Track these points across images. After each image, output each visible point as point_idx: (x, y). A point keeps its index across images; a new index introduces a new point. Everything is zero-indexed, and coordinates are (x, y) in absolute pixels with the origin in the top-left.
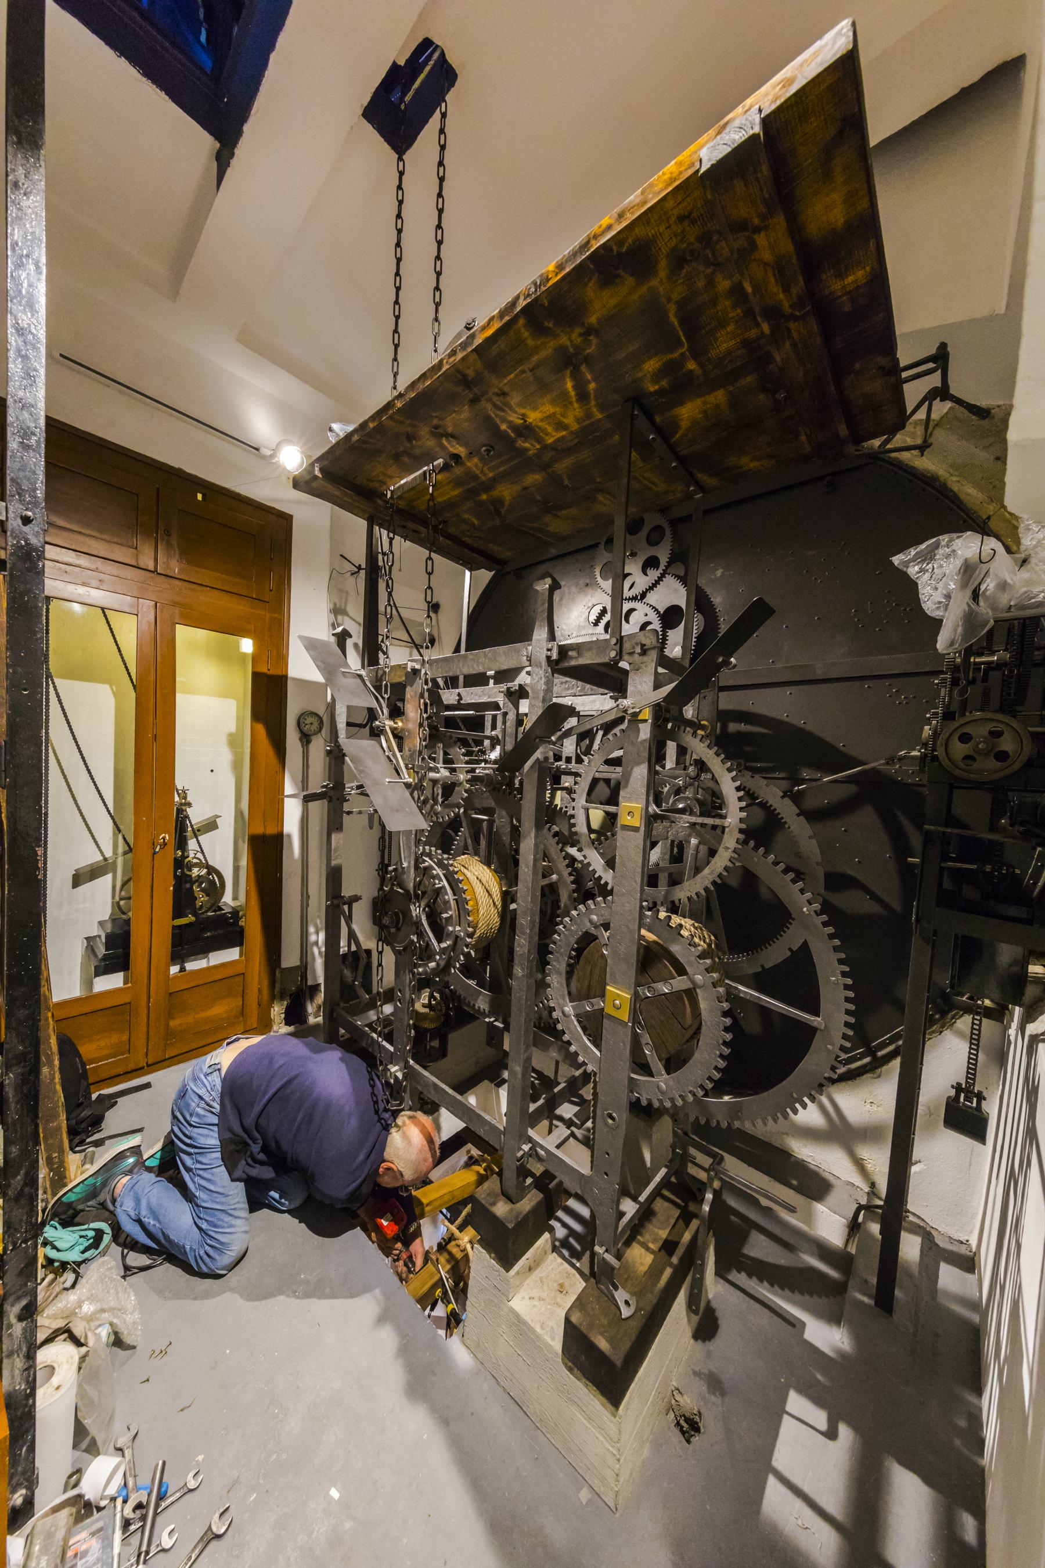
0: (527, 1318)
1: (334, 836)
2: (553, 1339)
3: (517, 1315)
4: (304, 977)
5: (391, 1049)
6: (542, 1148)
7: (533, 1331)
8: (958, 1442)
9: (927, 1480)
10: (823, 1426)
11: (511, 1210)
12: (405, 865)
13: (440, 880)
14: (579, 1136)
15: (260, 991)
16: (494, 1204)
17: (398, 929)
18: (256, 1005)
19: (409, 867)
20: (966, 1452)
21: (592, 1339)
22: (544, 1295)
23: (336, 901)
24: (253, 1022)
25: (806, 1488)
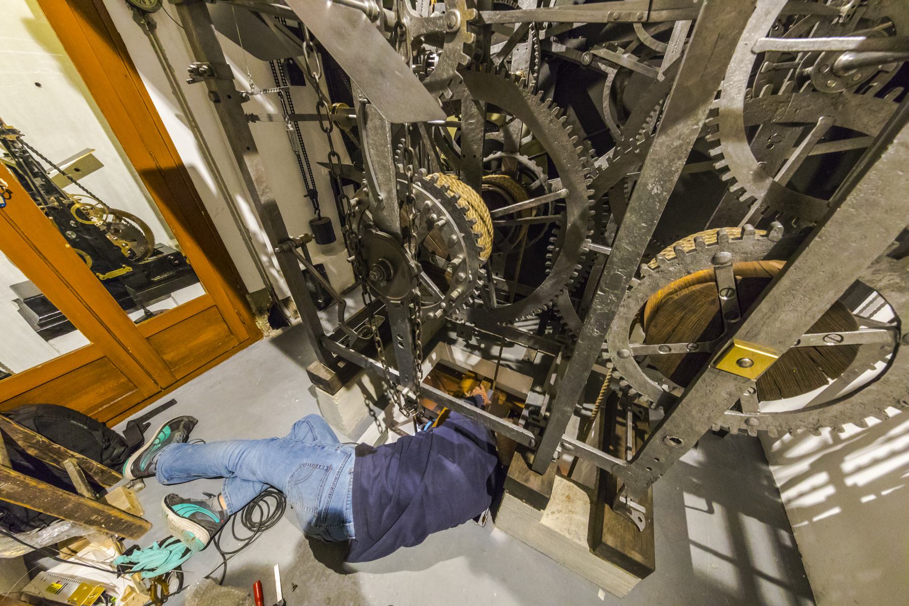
0: (557, 530)
1: (248, 160)
2: (580, 539)
3: (548, 528)
4: (274, 294)
5: (397, 373)
6: (570, 444)
7: (564, 537)
8: (766, 494)
9: (761, 519)
10: (706, 508)
11: (543, 481)
12: (382, 196)
13: (440, 213)
14: (514, 367)
15: (238, 314)
16: (527, 480)
17: (389, 280)
18: (241, 324)
19: (389, 198)
20: (771, 497)
21: (629, 555)
22: (560, 507)
23: (285, 247)
24: (243, 334)
25: (709, 546)
